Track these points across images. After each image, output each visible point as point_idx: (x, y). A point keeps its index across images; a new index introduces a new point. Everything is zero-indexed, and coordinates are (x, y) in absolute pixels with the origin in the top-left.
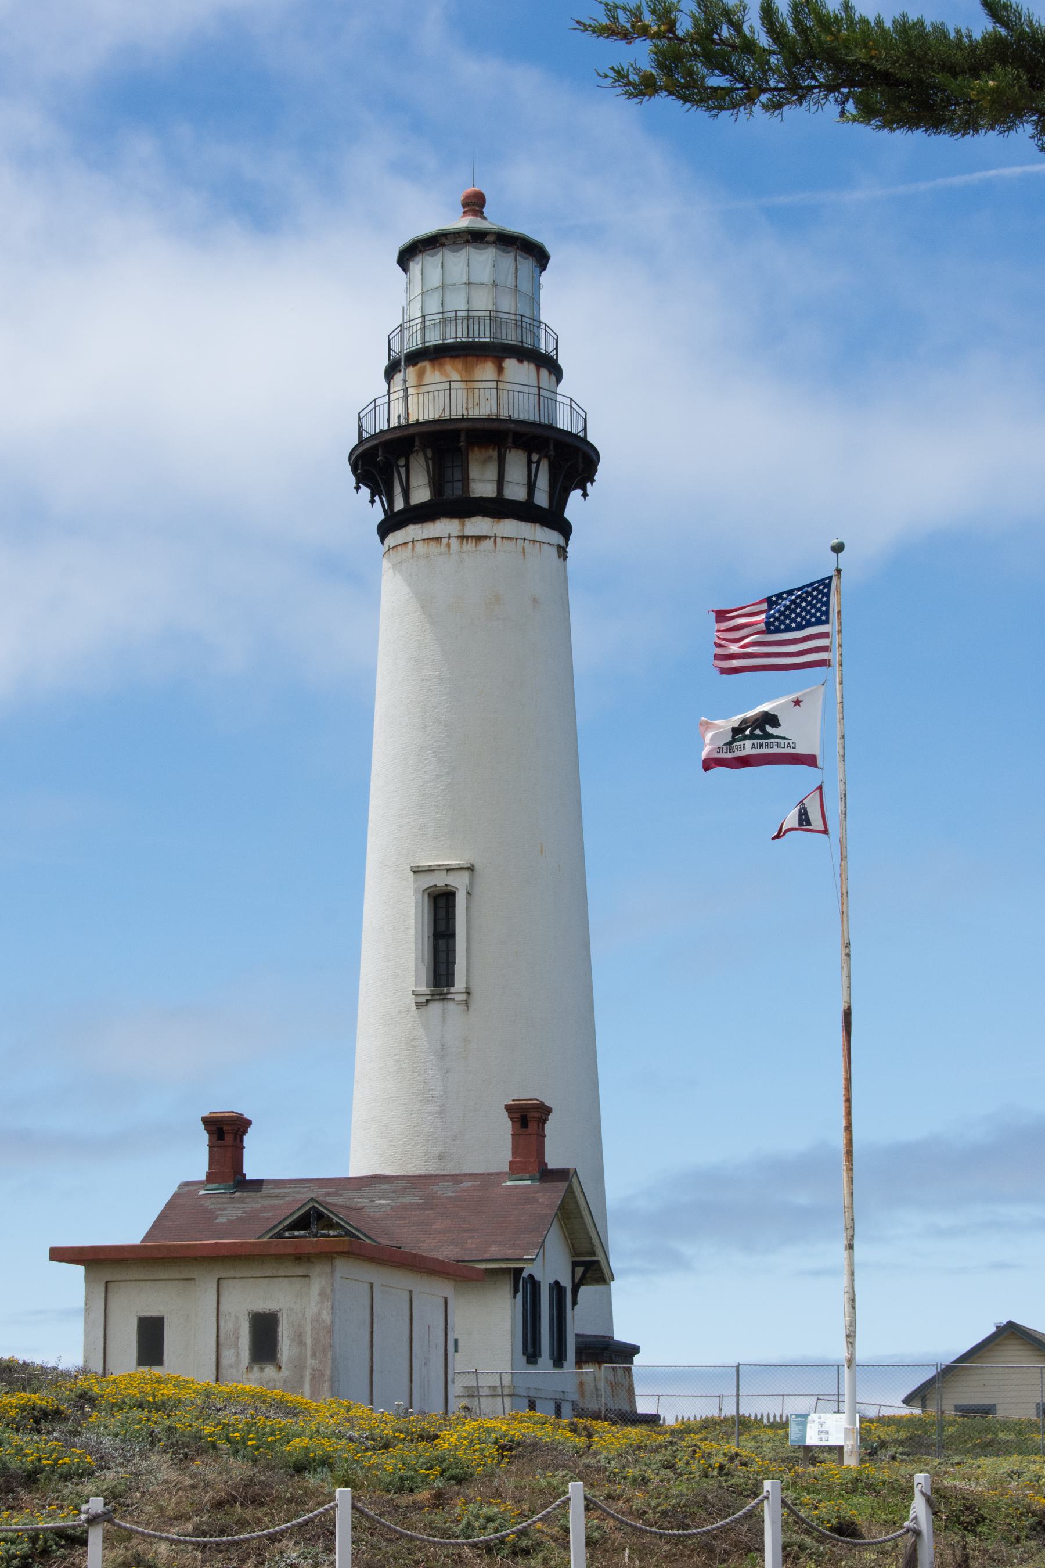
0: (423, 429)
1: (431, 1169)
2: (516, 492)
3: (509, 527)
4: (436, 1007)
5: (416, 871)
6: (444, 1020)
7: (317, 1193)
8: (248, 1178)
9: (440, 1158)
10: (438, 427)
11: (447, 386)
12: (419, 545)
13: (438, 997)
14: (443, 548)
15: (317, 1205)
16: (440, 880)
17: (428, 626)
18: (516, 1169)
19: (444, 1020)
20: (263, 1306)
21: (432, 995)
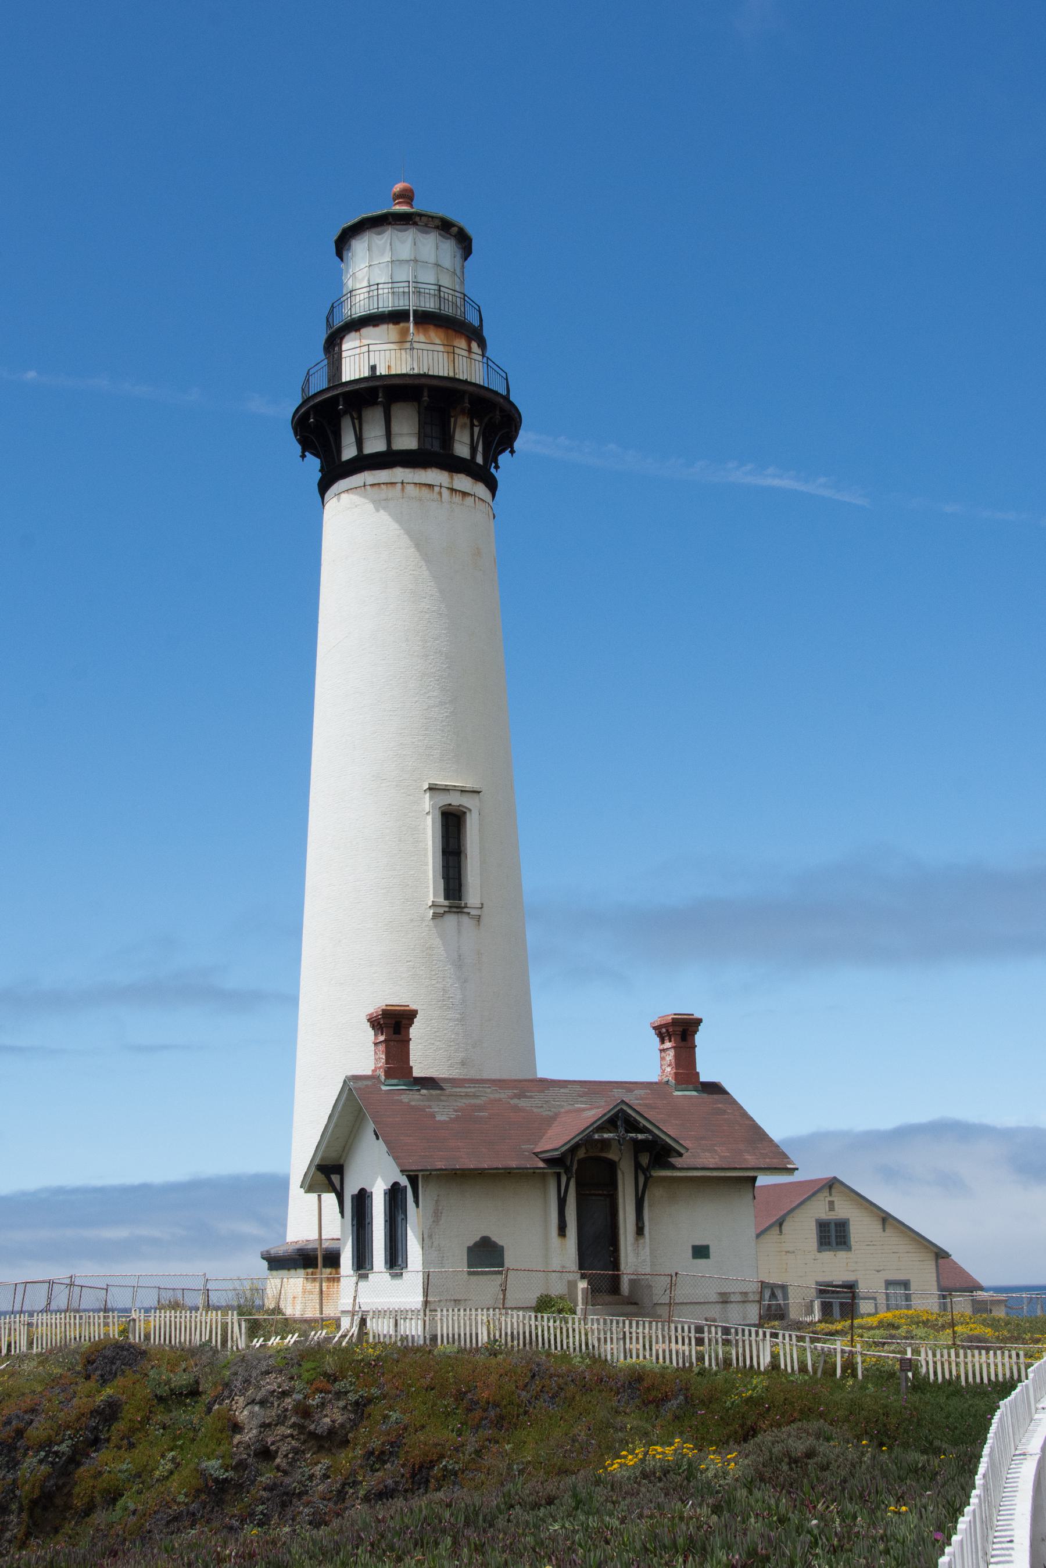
0: (435, 382)
1: (455, 1073)
2: (462, 450)
4: (451, 920)
5: (432, 789)
6: (459, 932)
7: (619, 1094)
8: (702, 1079)
9: (463, 1063)
10: (409, 381)
11: (366, 349)
12: (410, 488)
13: (455, 910)
14: (436, 496)
15: (625, 1108)
16: (455, 800)
17: (423, 563)
18: (389, 1073)
19: (459, 932)
20: (832, 1213)
21: (450, 907)
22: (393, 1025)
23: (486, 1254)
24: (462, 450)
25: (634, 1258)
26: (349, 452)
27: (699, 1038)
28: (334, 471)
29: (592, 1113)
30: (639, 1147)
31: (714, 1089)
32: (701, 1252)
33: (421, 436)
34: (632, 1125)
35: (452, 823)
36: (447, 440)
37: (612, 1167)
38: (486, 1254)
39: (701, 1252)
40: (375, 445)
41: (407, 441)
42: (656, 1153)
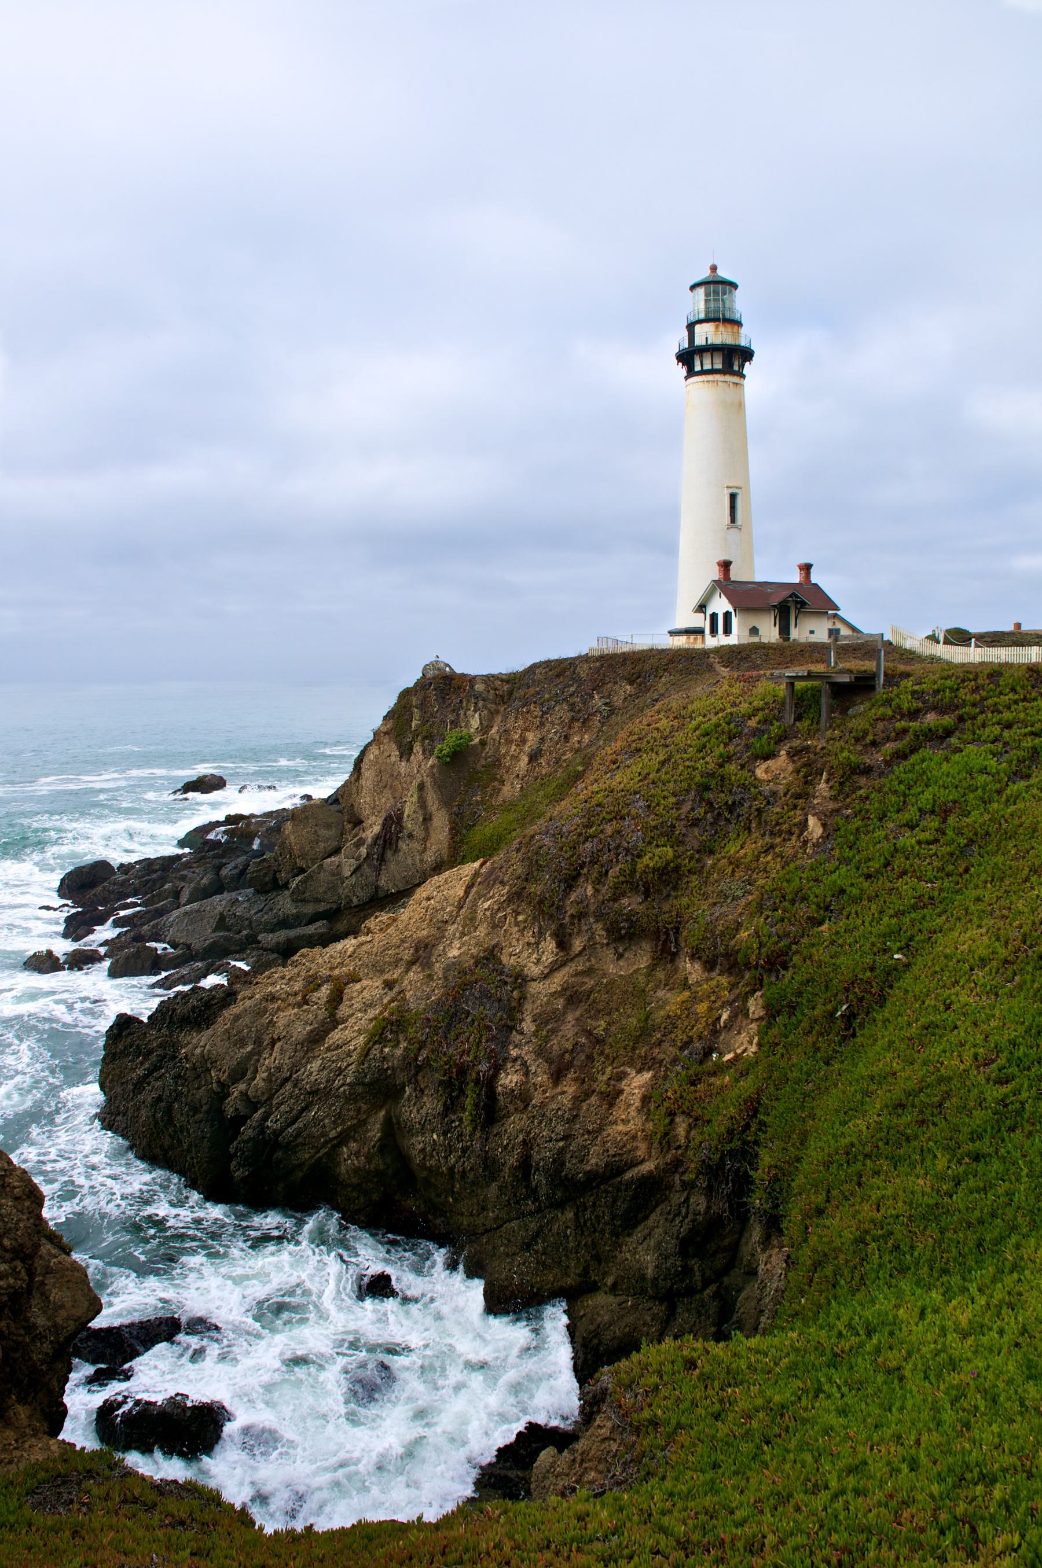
3: (736, 379)
16: (734, 491)
22: (725, 566)
23: (754, 631)
24: (736, 368)
25: (795, 634)
26: (698, 368)
27: (812, 570)
28: (691, 373)
29: (785, 594)
30: (797, 602)
31: (816, 585)
32: (812, 632)
33: (723, 364)
34: (797, 597)
35: (733, 497)
36: (731, 366)
37: (789, 608)
38: (754, 631)
39: (812, 632)
40: (707, 366)
41: (718, 366)
42: (803, 604)
